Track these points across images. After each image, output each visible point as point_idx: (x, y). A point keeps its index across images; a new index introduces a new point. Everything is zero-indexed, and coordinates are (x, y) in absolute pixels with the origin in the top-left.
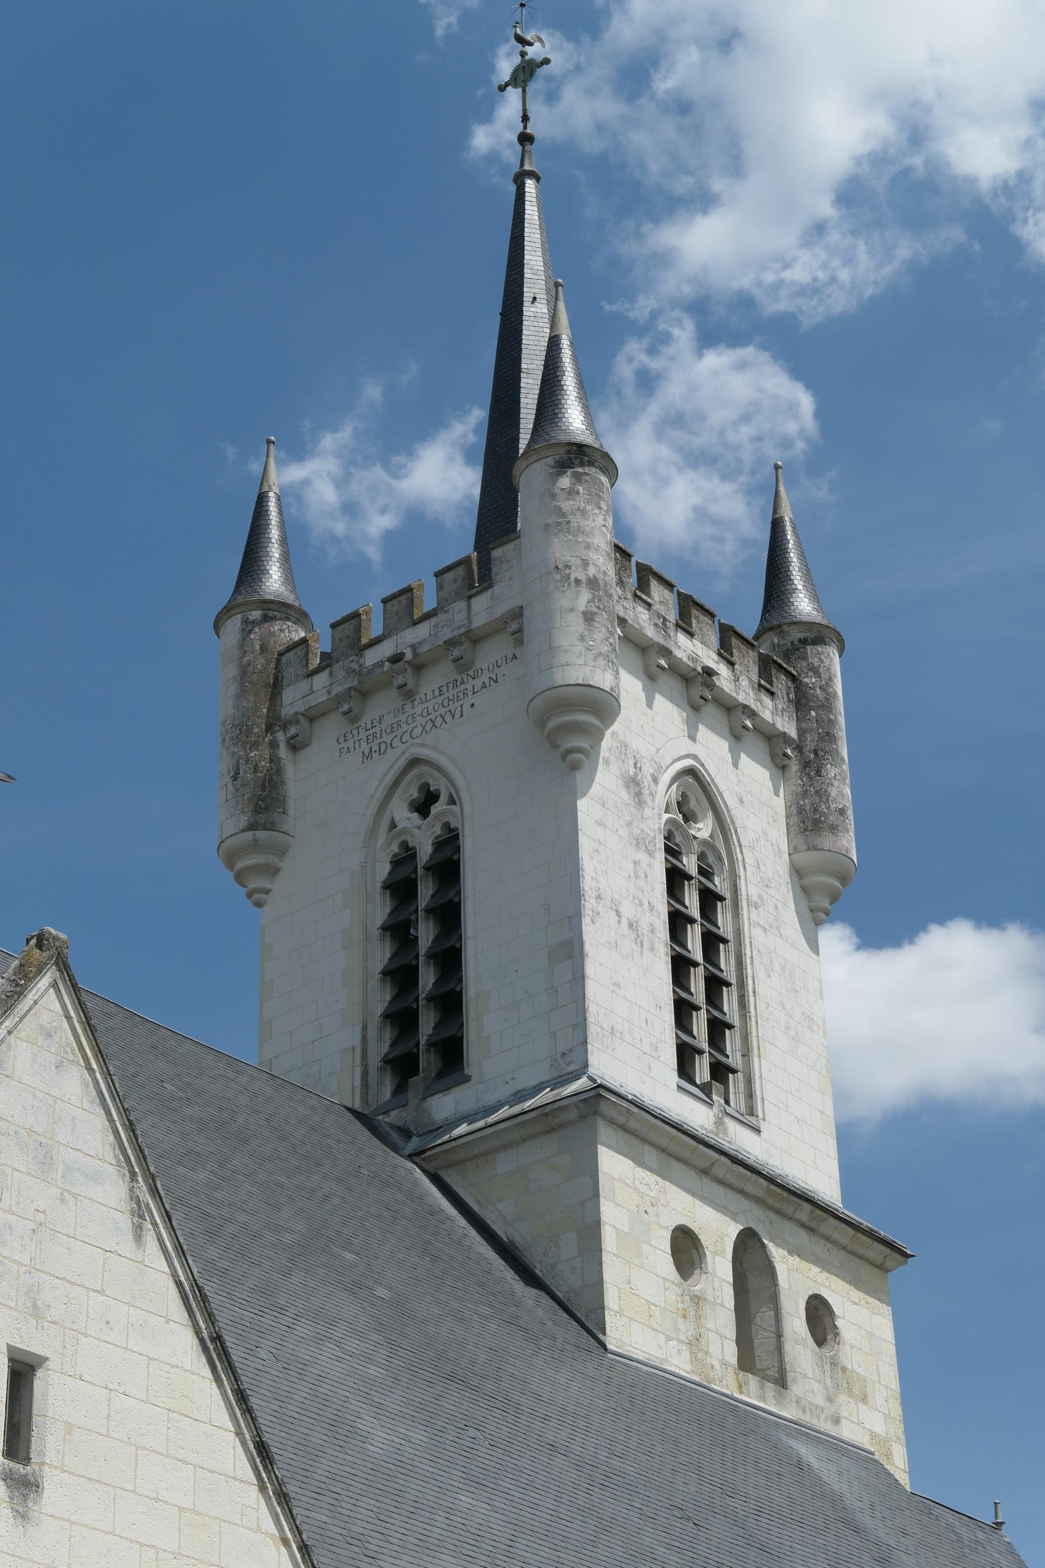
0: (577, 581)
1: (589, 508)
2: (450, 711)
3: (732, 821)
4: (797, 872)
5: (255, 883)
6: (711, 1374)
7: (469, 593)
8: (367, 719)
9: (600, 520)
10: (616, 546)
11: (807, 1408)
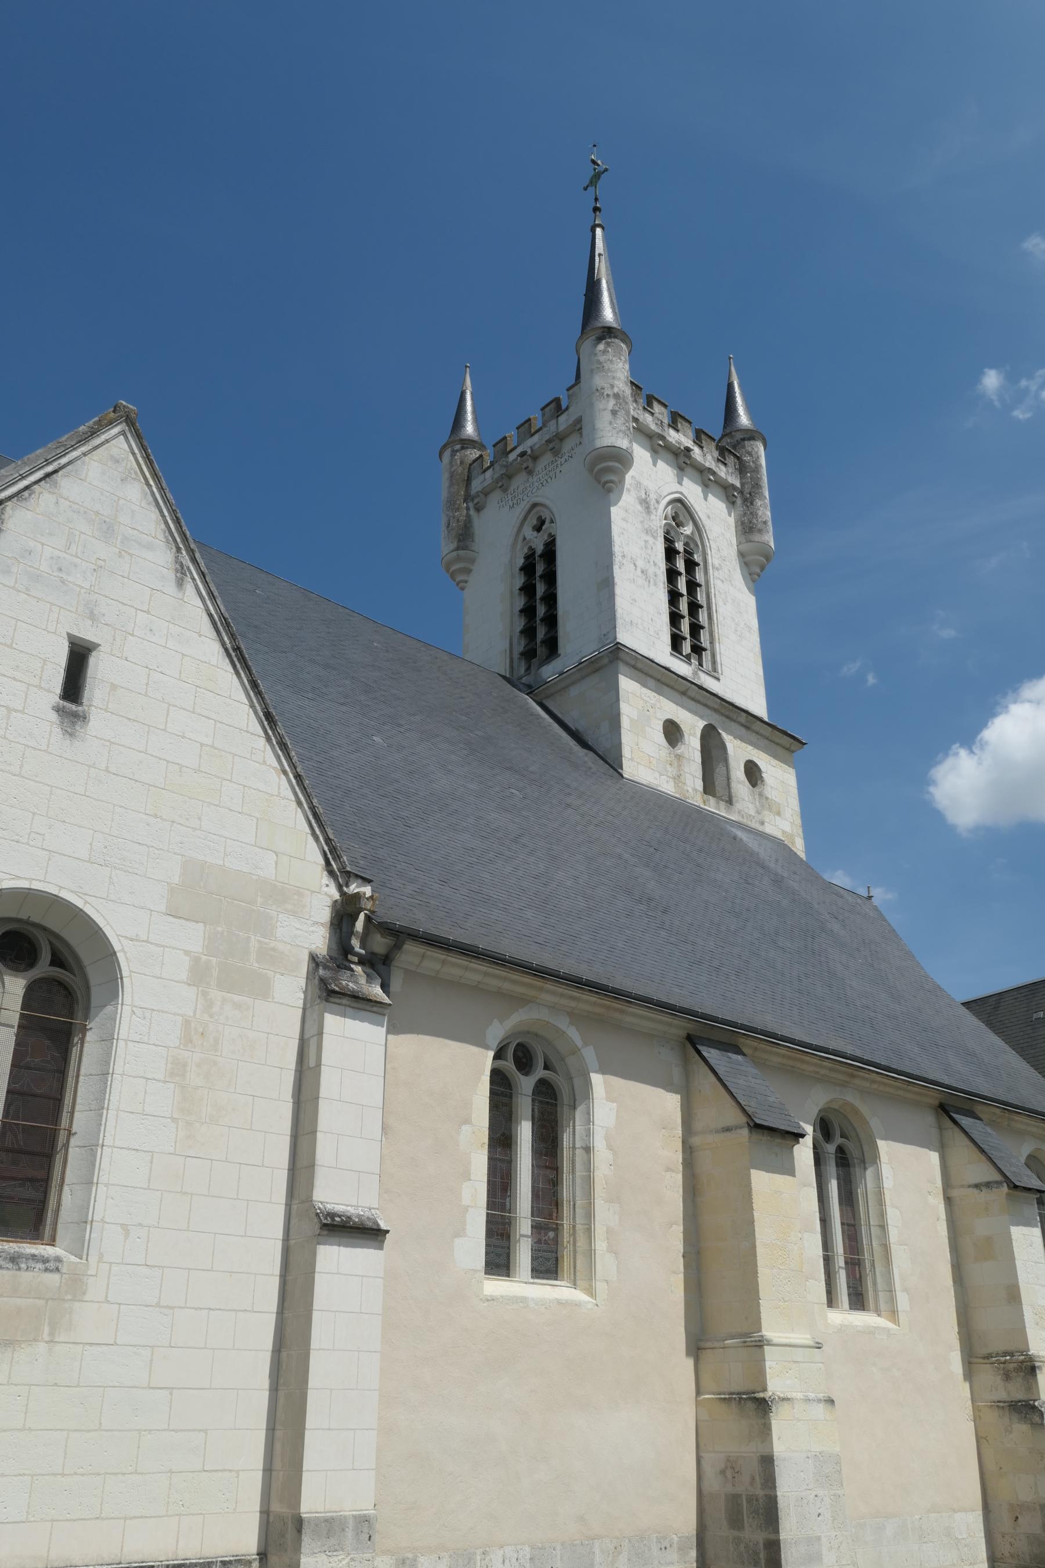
0: (608, 395)
1: (614, 359)
3: (704, 527)
4: (741, 555)
5: (459, 578)
6: (687, 795)
7: (557, 414)
8: (511, 489)
9: (621, 365)
10: (632, 383)
11: (745, 816)
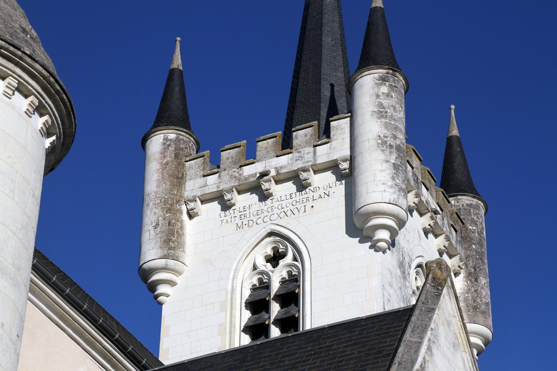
2: (297, 208)
7: (315, 144)
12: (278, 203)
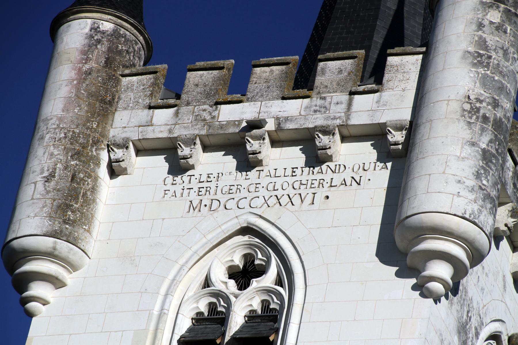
2: (300, 194)
7: (354, 89)
12: (269, 179)
